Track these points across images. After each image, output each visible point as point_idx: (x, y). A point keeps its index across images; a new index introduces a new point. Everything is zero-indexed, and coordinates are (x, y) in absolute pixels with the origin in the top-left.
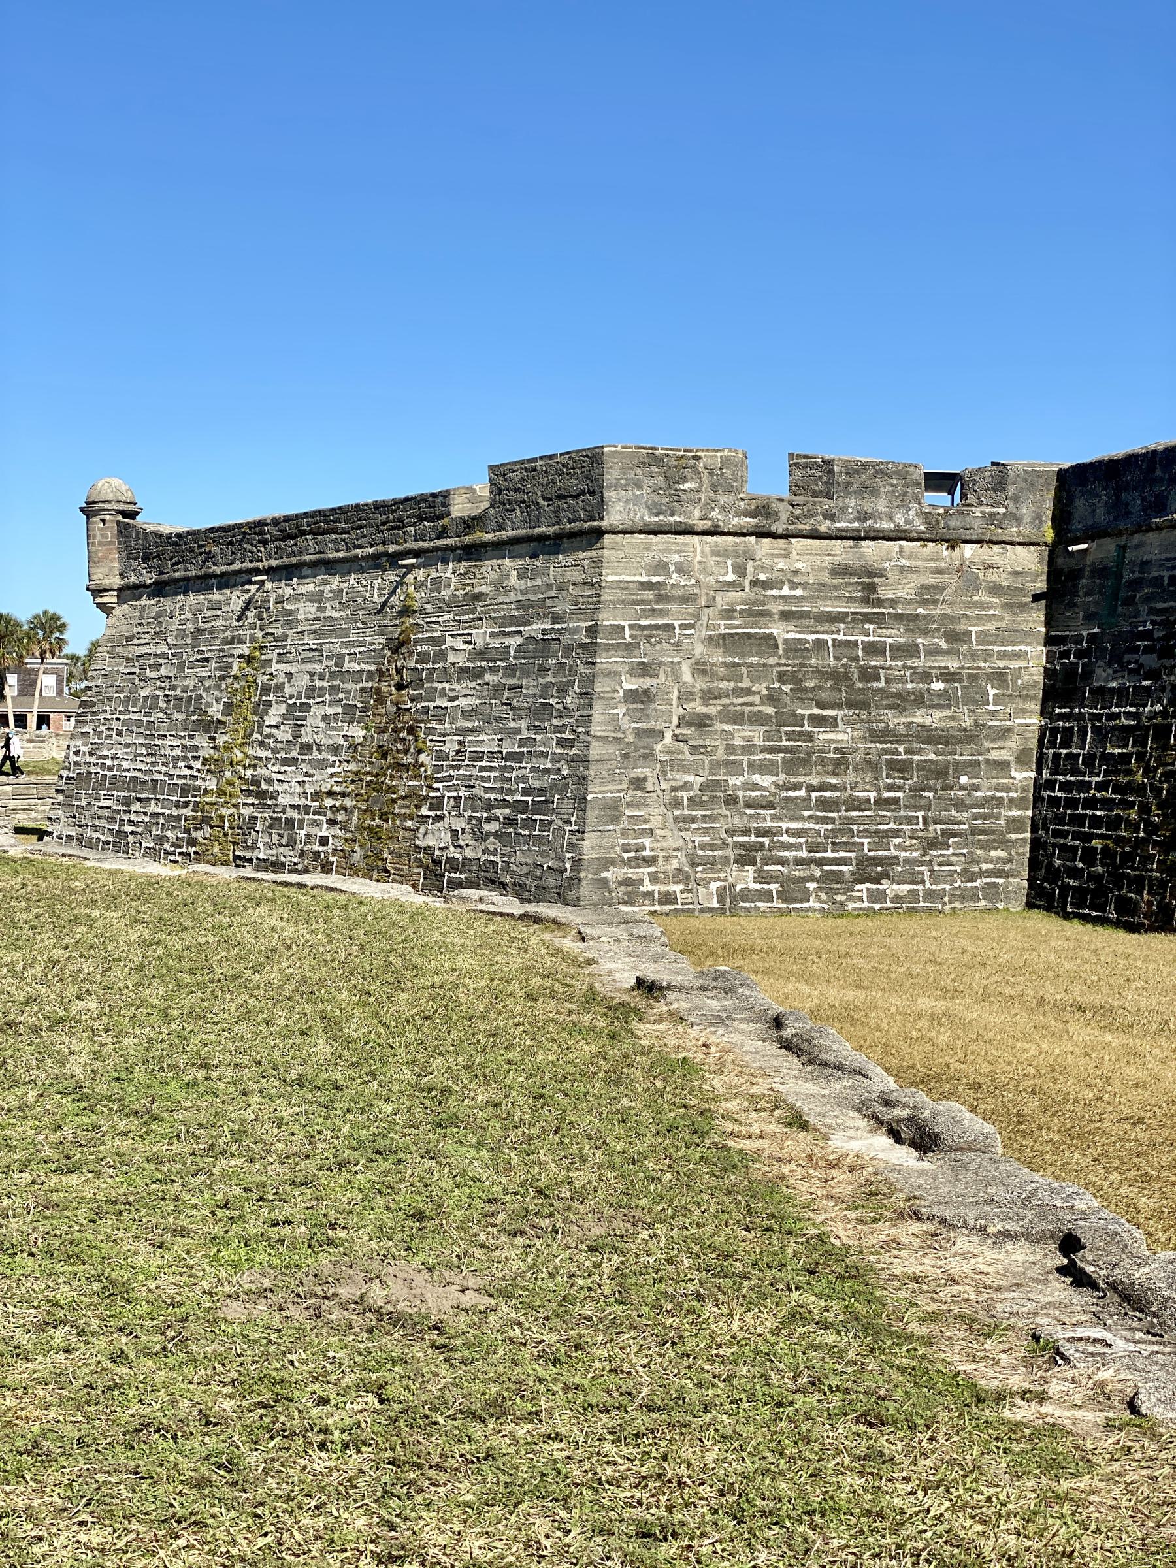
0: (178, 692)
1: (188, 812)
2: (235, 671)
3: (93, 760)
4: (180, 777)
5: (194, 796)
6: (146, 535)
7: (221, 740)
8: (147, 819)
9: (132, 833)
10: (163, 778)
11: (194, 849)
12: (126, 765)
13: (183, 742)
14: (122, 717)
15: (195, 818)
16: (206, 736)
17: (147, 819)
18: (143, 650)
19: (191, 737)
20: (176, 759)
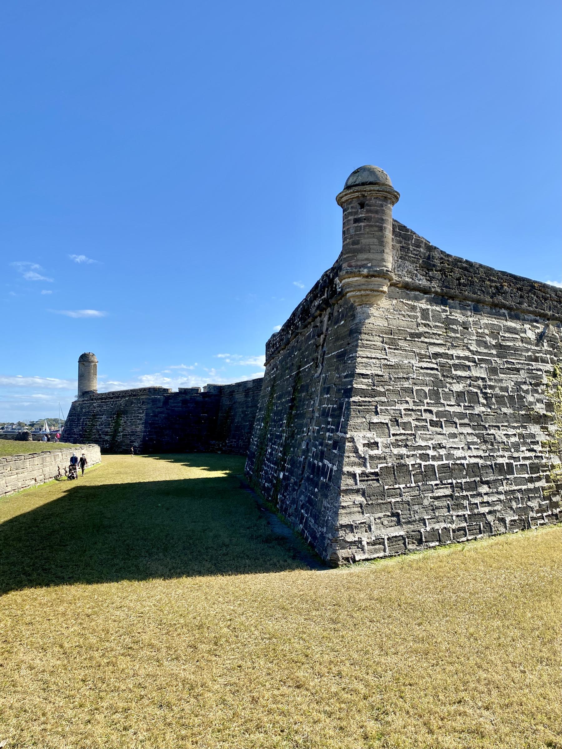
0: (497, 391)
1: (542, 483)
2: (545, 380)
3: (404, 451)
4: (525, 458)
5: (543, 471)
6: (430, 248)
7: (552, 428)
8: (502, 497)
9: (490, 512)
10: (507, 461)
11: (558, 510)
12: (458, 453)
13: (518, 431)
14: (434, 410)
15: (550, 488)
16: (538, 427)
17: (502, 497)
18: (441, 350)
19: (525, 427)
20: (516, 446)
